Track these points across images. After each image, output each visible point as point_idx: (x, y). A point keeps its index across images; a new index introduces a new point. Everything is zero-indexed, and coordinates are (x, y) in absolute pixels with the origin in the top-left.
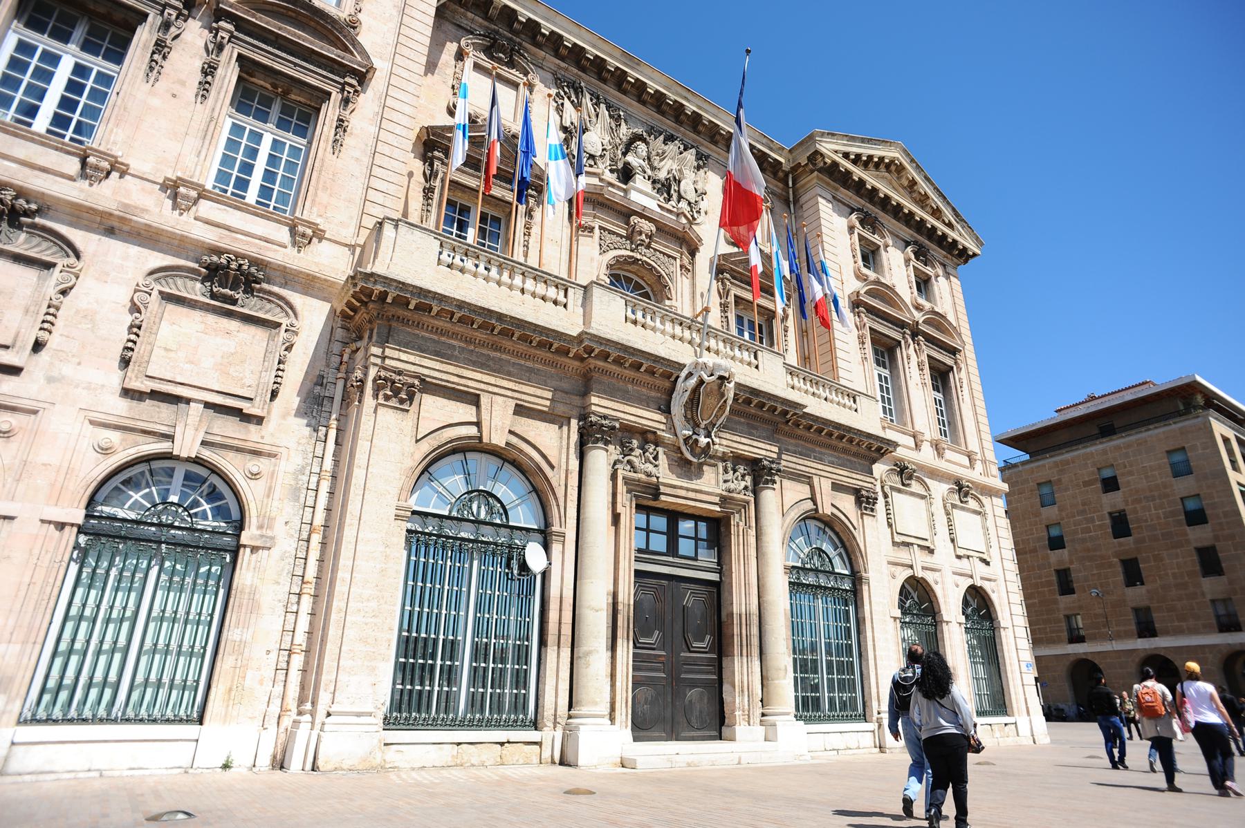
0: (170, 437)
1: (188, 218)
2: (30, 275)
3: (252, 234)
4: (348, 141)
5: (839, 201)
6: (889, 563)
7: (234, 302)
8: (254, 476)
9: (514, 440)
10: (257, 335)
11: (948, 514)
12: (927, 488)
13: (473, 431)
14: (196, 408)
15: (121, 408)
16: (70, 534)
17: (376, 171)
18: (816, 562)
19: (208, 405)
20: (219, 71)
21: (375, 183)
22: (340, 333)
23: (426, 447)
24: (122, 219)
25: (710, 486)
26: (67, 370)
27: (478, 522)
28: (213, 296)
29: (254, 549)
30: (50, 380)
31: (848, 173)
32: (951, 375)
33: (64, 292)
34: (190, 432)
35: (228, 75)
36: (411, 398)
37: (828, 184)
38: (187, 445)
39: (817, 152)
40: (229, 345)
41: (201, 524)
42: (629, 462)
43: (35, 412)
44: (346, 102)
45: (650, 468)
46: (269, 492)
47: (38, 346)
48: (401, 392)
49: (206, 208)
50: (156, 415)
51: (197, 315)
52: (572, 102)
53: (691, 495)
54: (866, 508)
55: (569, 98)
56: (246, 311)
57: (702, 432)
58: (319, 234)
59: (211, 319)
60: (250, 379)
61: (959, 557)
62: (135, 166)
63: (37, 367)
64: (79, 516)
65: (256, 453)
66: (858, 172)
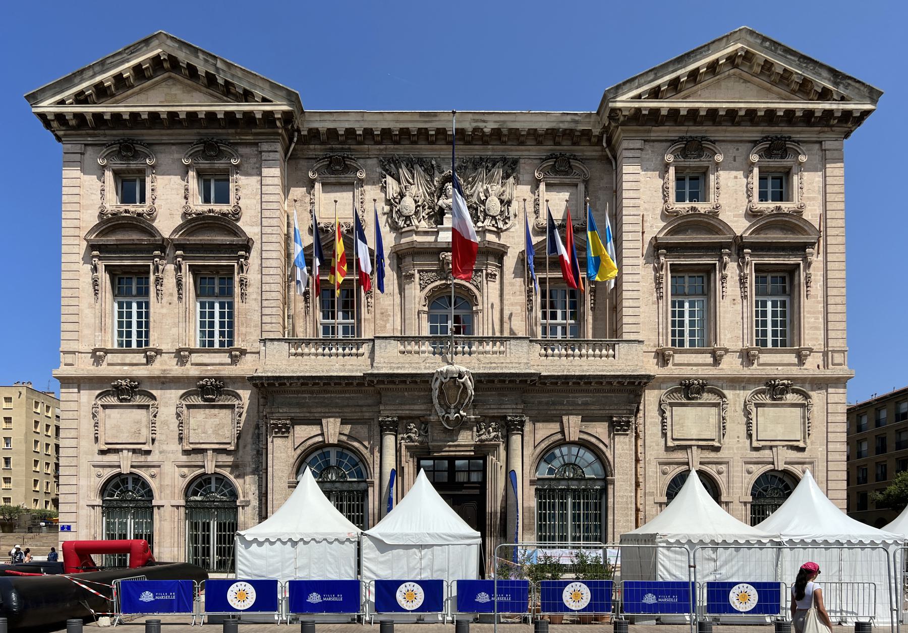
0: (203, 467)
2: (144, 411)
3: (216, 364)
4: (250, 290)
5: (654, 141)
6: (660, 464)
7: (213, 400)
10: (226, 413)
11: (747, 413)
12: (722, 396)
14: (210, 453)
15: (185, 458)
16: (182, 510)
17: (265, 303)
18: (569, 474)
19: (214, 450)
20: (184, 280)
21: (265, 311)
22: (261, 400)
24: (165, 377)
26: (165, 447)
27: (335, 482)
28: (206, 400)
29: (243, 507)
30: (161, 452)
32: (797, 274)
33: (155, 416)
34: (210, 463)
35: (188, 280)
37: (637, 131)
38: (210, 468)
39: (614, 110)
40: (217, 421)
42: (409, 437)
43: (159, 466)
44: (241, 268)
48: (284, 431)
49: (195, 358)
50: (197, 459)
51: (202, 411)
53: (452, 449)
54: (618, 430)
56: (220, 403)
57: (453, 411)
58: (243, 352)
59: (207, 411)
60: (228, 434)
61: (757, 449)
62: (164, 347)
63: (155, 448)
64: (182, 502)
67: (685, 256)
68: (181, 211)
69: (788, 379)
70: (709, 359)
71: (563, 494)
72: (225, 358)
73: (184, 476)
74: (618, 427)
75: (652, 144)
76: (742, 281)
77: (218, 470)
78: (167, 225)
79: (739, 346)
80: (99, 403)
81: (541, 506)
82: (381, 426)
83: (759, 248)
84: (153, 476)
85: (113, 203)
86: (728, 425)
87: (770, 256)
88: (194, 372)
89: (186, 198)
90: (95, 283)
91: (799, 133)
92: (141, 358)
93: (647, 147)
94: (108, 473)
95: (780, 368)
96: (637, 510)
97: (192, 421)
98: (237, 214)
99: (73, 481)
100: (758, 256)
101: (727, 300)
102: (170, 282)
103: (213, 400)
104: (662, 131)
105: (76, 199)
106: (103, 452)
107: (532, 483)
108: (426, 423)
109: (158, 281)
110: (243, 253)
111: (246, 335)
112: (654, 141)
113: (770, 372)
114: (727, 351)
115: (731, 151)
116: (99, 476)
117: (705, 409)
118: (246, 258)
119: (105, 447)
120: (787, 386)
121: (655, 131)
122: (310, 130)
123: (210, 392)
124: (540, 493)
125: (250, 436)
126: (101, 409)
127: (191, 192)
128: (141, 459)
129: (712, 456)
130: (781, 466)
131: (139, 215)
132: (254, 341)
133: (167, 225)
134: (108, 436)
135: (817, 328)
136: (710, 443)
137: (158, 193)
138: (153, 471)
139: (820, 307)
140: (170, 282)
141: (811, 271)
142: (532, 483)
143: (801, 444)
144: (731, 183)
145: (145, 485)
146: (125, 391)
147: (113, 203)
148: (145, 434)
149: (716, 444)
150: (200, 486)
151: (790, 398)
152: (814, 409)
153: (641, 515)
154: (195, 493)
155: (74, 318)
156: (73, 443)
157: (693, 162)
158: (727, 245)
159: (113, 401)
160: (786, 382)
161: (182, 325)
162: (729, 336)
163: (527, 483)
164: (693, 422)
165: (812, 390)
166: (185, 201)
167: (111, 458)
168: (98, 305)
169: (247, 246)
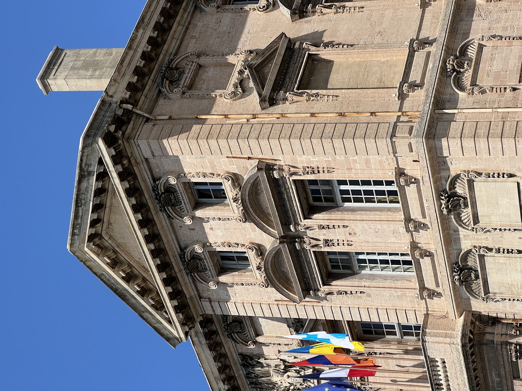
5: (197, 290)
67: (312, 273)
69: (439, 199)
75: (201, 292)
83: (286, 218)
87: (292, 206)
91: (145, 181)
93: (205, 295)
95: (426, 205)
100: (294, 216)
104: (187, 289)
112: (197, 290)
115: (185, 232)
121: (189, 293)
157: (209, 263)
165: (448, 169)
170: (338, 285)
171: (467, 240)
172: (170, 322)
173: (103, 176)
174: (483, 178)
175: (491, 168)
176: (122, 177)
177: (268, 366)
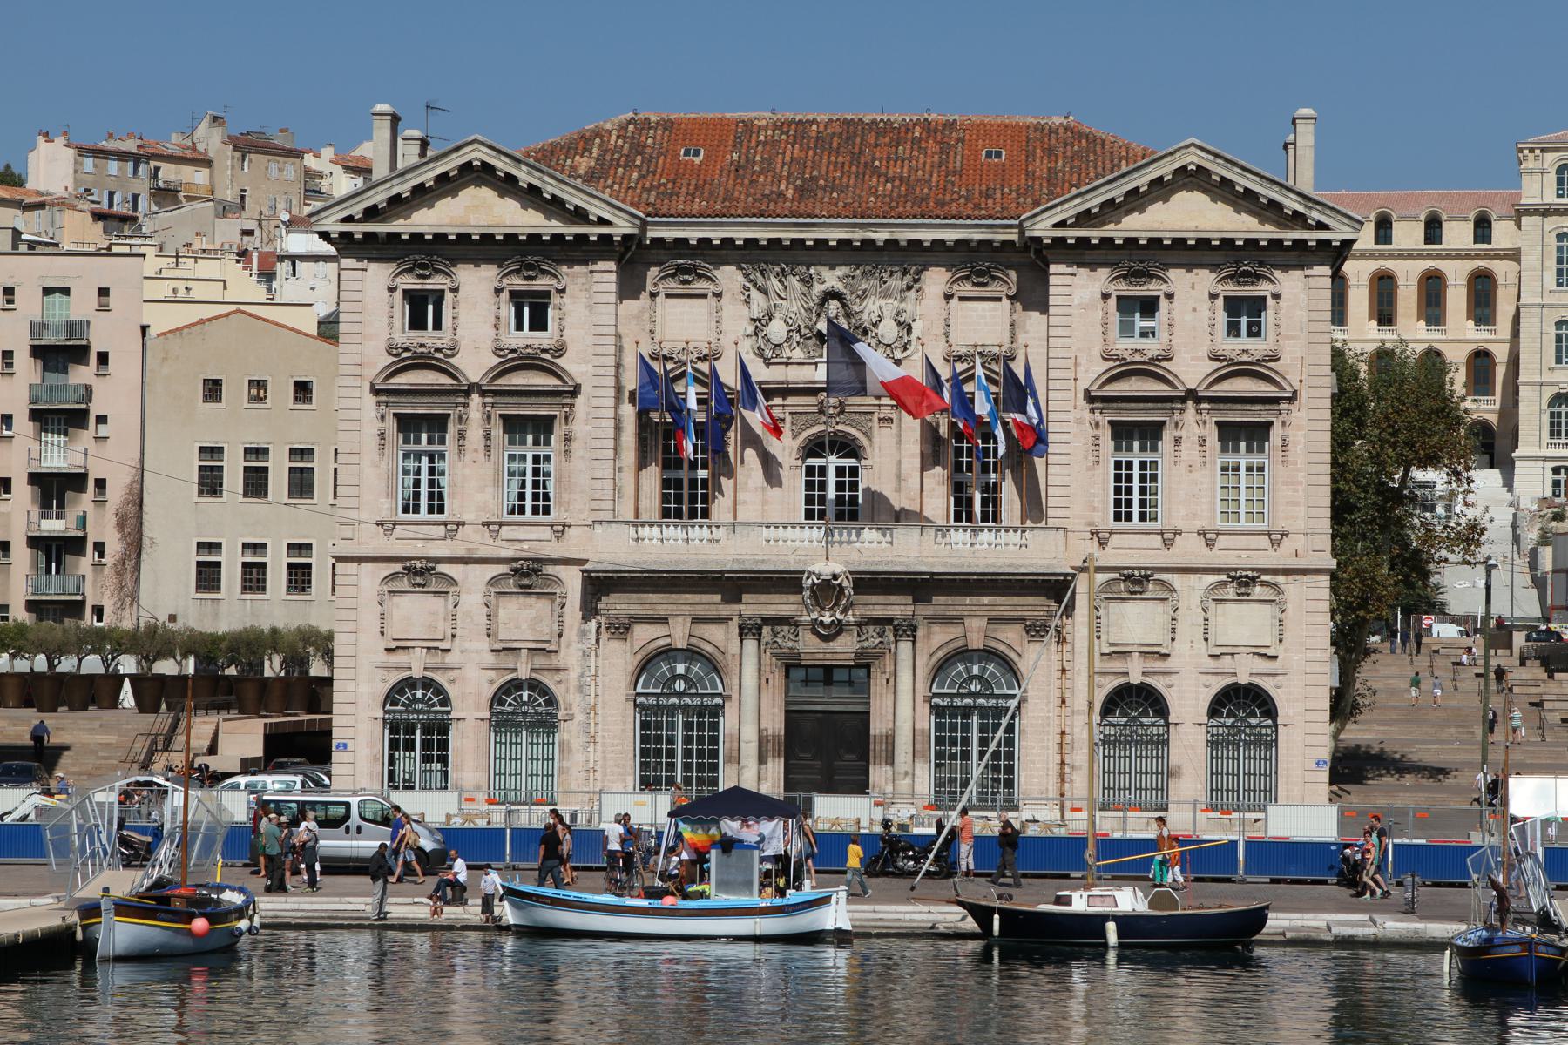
1: (498, 542)
2: (440, 600)
3: (531, 538)
4: (575, 445)
7: (529, 587)
8: (559, 683)
9: (694, 641)
13: (667, 641)
18: (976, 687)
23: (639, 657)
25: (845, 648)
26: (467, 645)
27: (680, 695)
28: (521, 587)
31: (1083, 242)
35: (497, 431)
36: (627, 629)
38: (524, 673)
40: (532, 613)
41: (540, 709)
44: (566, 418)
45: (790, 644)
46: (567, 691)
47: (454, 636)
49: (506, 532)
50: (508, 660)
52: (759, 289)
55: (755, 285)
59: (522, 600)
62: (467, 517)
64: (487, 715)
65: (558, 670)
66: (1094, 234)
68: (488, 345)
69: (1252, 570)
70: (1157, 541)
71: (967, 712)
72: (546, 533)
73: (492, 682)
74: (1036, 631)
76: (1202, 441)
77: (534, 675)
78: (475, 364)
79: (1199, 525)
80: (386, 588)
81: (939, 727)
82: (741, 628)
84: (453, 681)
85: (404, 336)
86: (1179, 628)
88: (506, 553)
89: (496, 327)
90: (382, 435)
92: (441, 531)
94: (395, 677)
96: (1063, 733)
97: (501, 612)
98: (560, 350)
99: (351, 686)
101: (1183, 466)
102: (475, 434)
103: (529, 587)
105: (357, 328)
106: (388, 650)
107: (927, 699)
108: (797, 624)
109: (462, 435)
110: (568, 401)
111: (570, 502)
113: (1231, 560)
114: (1177, 533)
116: (384, 681)
117: (1151, 604)
118: (571, 406)
119: (393, 645)
120: (1253, 579)
122: (653, 240)
123: (528, 575)
124: (938, 711)
125: (575, 632)
126: (387, 596)
127: (502, 320)
128: (437, 659)
129: (1159, 665)
130: (1243, 679)
131: (437, 350)
132: (581, 511)
133: (475, 364)
134: (395, 630)
135: (1296, 504)
136: (1156, 649)
137: (462, 319)
138: (451, 675)
139: (1301, 476)
140: (475, 434)
141: (1290, 432)
142: (927, 699)
143: (1270, 652)
144: (1189, 317)
145: (439, 690)
146: (420, 573)
147: (404, 336)
148: (443, 628)
149: (1164, 651)
150: (508, 694)
151: (1258, 591)
152: (1289, 607)
153: (1068, 739)
154: (501, 703)
155: (354, 480)
156: (351, 638)
158: (1183, 400)
159: (404, 584)
160: (1250, 573)
161: (490, 490)
162: (1183, 512)
163: (919, 699)
164: (1135, 621)
166: (494, 331)
167: (400, 658)
168: (384, 465)
169: (575, 392)
170: (1106, 434)
171: (1191, 590)
172: (1061, 224)
173: (1298, 219)
174: (1278, 615)
175: (1288, 624)
176: (1300, 244)
177: (903, 300)
